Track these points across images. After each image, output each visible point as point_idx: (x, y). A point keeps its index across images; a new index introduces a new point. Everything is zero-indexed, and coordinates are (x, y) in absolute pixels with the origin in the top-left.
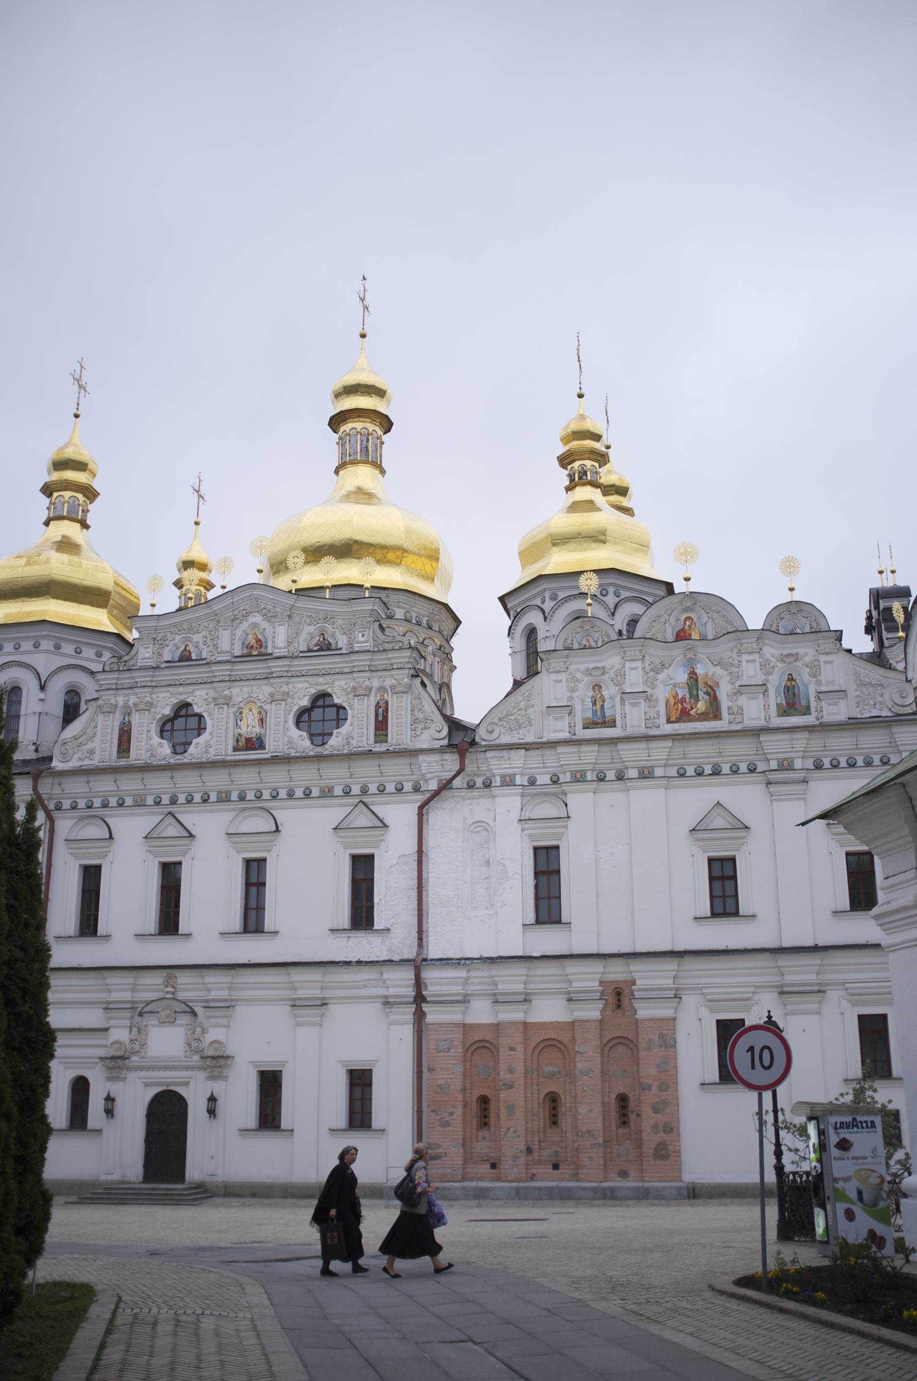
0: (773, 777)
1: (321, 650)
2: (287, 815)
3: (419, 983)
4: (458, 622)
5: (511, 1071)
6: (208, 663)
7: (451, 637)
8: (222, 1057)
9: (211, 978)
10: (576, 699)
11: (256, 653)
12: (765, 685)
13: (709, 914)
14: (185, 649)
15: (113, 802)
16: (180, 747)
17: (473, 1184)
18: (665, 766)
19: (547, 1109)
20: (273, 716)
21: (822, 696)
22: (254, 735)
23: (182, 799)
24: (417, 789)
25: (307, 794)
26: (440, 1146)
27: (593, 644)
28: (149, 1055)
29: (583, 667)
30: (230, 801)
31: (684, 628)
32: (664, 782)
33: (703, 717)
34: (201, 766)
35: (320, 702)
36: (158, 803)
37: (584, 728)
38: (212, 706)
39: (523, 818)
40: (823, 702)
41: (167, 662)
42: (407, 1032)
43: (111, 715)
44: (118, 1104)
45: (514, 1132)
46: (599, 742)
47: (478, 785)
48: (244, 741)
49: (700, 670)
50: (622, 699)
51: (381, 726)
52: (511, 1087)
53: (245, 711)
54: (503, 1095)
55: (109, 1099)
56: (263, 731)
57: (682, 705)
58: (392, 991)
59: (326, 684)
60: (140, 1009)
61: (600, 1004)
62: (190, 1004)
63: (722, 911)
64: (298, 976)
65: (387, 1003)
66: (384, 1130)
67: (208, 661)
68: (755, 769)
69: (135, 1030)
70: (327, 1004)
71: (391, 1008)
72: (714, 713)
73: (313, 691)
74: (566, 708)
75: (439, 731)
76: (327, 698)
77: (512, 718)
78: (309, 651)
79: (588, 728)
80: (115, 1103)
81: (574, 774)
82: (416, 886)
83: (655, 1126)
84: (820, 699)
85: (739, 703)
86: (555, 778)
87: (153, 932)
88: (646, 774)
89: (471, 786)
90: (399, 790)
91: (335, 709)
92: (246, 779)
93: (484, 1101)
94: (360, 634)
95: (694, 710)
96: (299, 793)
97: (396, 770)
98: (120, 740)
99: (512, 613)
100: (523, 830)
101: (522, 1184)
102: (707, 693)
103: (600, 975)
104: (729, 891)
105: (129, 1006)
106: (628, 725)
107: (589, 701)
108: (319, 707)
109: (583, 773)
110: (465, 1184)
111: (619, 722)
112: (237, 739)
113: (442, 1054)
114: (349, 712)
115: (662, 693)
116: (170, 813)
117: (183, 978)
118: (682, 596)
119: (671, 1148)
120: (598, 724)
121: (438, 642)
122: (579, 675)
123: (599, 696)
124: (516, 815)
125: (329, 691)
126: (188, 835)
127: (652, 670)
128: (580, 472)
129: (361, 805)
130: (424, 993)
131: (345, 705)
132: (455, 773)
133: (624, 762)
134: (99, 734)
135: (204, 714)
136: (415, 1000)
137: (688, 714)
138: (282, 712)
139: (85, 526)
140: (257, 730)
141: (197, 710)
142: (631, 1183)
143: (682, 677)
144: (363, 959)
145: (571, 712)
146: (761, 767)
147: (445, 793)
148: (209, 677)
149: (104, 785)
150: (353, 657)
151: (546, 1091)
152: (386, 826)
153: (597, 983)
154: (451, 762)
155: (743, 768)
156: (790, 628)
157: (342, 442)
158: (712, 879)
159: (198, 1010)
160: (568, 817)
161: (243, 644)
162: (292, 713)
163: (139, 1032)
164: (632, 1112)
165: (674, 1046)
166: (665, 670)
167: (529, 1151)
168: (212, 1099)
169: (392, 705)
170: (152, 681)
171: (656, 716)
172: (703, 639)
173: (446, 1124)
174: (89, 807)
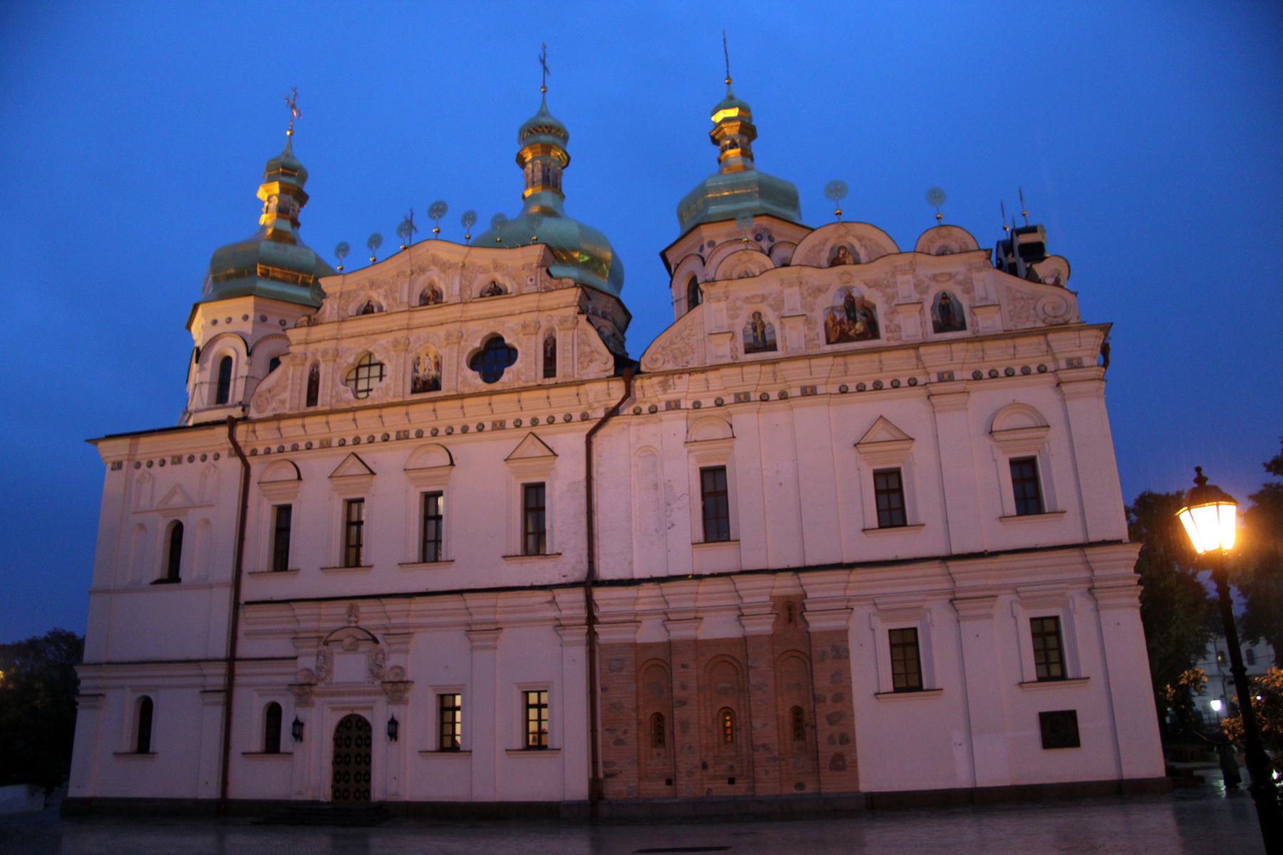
0: (934, 389)
2: (464, 448)
3: (590, 603)
5: (684, 687)
8: (402, 682)
9: (392, 606)
12: (920, 303)
13: (876, 525)
14: (368, 304)
15: (302, 445)
21: (977, 311)
23: (364, 439)
24: (585, 418)
25: (481, 428)
27: (751, 275)
28: (334, 681)
32: (826, 399)
33: (861, 337)
36: (342, 443)
38: (392, 353)
39: (688, 440)
42: (580, 653)
45: (690, 748)
47: (643, 412)
48: (421, 383)
49: (855, 294)
50: (781, 323)
53: (423, 356)
54: (676, 712)
56: (439, 374)
57: (841, 327)
58: (565, 613)
60: (324, 639)
61: (772, 619)
62: (372, 632)
64: (472, 600)
65: (559, 625)
66: (559, 749)
69: (321, 657)
70: (501, 629)
71: (564, 629)
72: (872, 330)
73: (486, 333)
74: (728, 335)
75: (606, 363)
77: (674, 346)
78: (481, 296)
81: (737, 396)
82: (585, 511)
83: (831, 740)
84: (974, 314)
85: (896, 322)
86: (719, 402)
87: (337, 565)
88: (809, 392)
89: (637, 412)
90: (568, 419)
92: (422, 415)
93: (659, 718)
94: (529, 279)
95: (853, 331)
96: (473, 428)
97: (563, 401)
100: (689, 452)
102: (864, 315)
104: (895, 504)
105: (314, 635)
106: (789, 348)
107: (750, 327)
109: (747, 395)
111: (779, 346)
113: (615, 673)
115: (820, 317)
116: (353, 453)
117: (365, 607)
123: (759, 322)
124: (682, 437)
126: (367, 472)
127: (810, 295)
129: (531, 436)
130: (596, 614)
132: (619, 401)
133: (786, 382)
134: (290, 386)
135: (385, 361)
138: (455, 354)
139: (295, 223)
140: (433, 372)
144: (535, 584)
145: (732, 339)
147: (614, 420)
152: (556, 455)
153: (767, 598)
154: (618, 389)
158: (878, 492)
159: (379, 637)
160: (734, 437)
162: (466, 354)
164: (806, 725)
165: (847, 657)
166: (822, 295)
167: (705, 766)
168: (393, 723)
171: (816, 337)
172: (857, 262)
173: (619, 742)
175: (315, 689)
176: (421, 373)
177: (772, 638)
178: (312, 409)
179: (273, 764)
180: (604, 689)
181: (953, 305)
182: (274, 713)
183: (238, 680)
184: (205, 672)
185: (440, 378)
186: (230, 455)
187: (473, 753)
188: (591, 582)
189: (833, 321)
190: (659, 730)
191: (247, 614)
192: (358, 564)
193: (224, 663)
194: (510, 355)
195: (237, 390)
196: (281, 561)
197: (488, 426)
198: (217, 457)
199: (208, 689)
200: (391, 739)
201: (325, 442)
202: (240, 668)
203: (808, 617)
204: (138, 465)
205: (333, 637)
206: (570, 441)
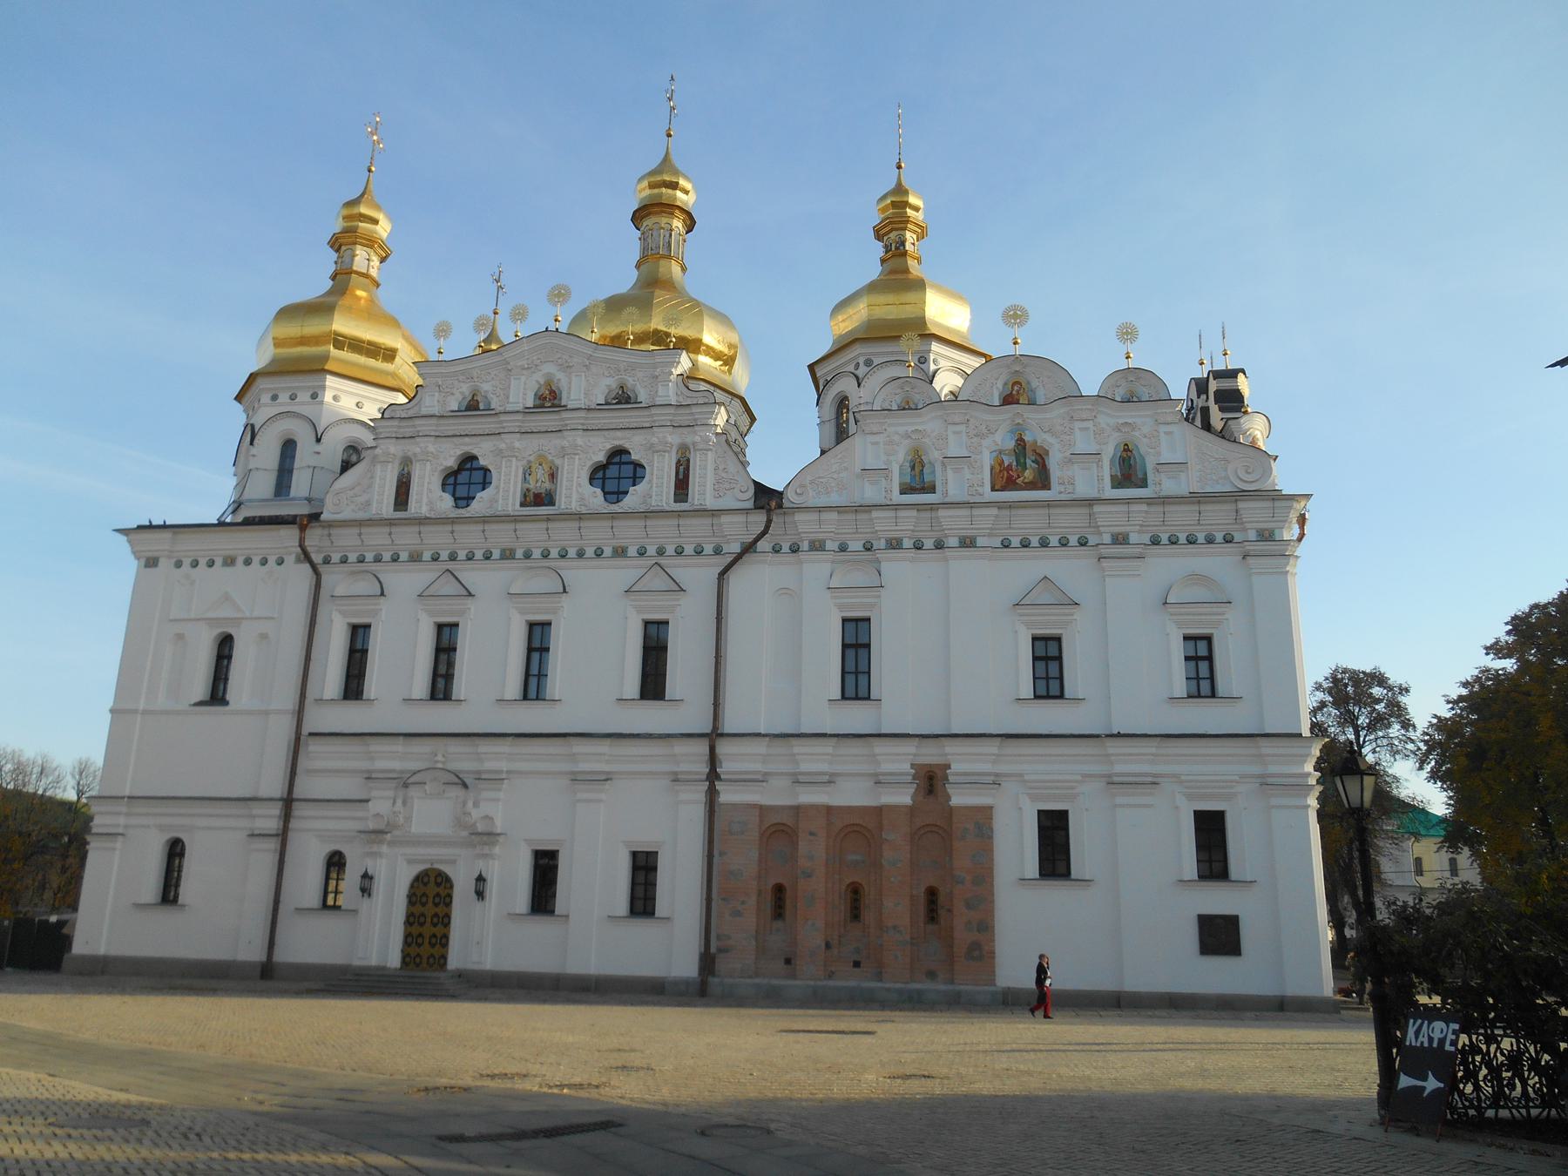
0: (1104, 551)
1: (616, 404)
2: (579, 575)
3: (713, 759)
4: (753, 419)
7: (746, 435)
8: (490, 834)
9: (485, 747)
10: (894, 463)
11: (549, 405)
15: (387, 556)
16: (463, 500)
17: (765, 981)
18: (990, 535)
20: (565, 472)
22: (543, 491)
23: (462, 555)
24: (718, 551)
25: (599, 553)
27: (913, 406)
29: (901, 429)
30: (514, 559)
31: (1011, 393)
33: (1031, 486)
34: (484, 520)
35: (617, 459)
36: (435, 558)
41: (453, 411)
44: (376, 880)
46: (918, 507)
48: (532, 498)
49: (1028, 438)
50: (943, 464)
51: (682, 486)
52: (809, 876)
53: (534, 466)
55: (366, 877)
56: (553, 487)
57: (1008, 473)
58: (684, 767)
59: (622, 439)
62: (461, 776)
63: (1045, 694)
64: (580, 747)
65: (676, 779)
66: (668, 918)
67: (498, 412)
68: (1087, 542)
69: (399, 802)
70: (611, 779)
72: (1042, 480)
73: (609, 446)
76: (623, 456)
78: (607, 404)
79: (905, 494)
80: (373, 881)
88: (968, 543)
89: (776, 550)
90: (699, 552)
91: (632, 466)
92: (533, 535)
96: (590, 552)
97: (696, 530)
101: (819, 983)
103: (912, 757)
104: (1054, 672)
107: (908, 465)
110: (757, 981)
112: (525, 494)
115: (987, 461)
116: (448, 570)
118: (1013, 358)
122: (896, 438)
123: (918, 460)
126: (465, 593)
128: (897, 243)
131: (644, 462)
136: (707, 777)
137: (1014, 483)
140: (547, 485)
141: (482, 462)
143: (1011, 444)
146: (1092, 540)
148: (497, 428)
149: (377, 539)
150: (654, 411)
151: (848, 881)
153: (906, 767)
155: (1073, 540)
157: (643, 239)
158: (1035, 659)
161: (535, 395)
162: (586, 468)
163: (404, 803)
167: (828, 946)
168: (480, 879)
169: (695, 463)
170: (435, 431)
172: (1032, 403)
173: (737, 913)
174: (362, 562)
175: (388, 837)
176: (532, 486)
177: (912, 811)
179: (329, 924)
180: (721, 854)
181: (1135, 458)
182: (336, 862)
183: (293, 824)
184: (255, 812)
185: (556, 491)
186: (298, 561)
188: (714, 736)
189: (1000, 465)
190: (779, 901)
191: (313, 748)
192: (447, 697)
193: (281, 803)
194: (637, 472)
195: (300, 484)
196: (353, 686)
197: (608, 551)
198: (280, 562)
199: (256, 832)
200: (478, 899)
202: (299, 810)
203: (950, 790)
204: (179, 564)
206: (699, 577)
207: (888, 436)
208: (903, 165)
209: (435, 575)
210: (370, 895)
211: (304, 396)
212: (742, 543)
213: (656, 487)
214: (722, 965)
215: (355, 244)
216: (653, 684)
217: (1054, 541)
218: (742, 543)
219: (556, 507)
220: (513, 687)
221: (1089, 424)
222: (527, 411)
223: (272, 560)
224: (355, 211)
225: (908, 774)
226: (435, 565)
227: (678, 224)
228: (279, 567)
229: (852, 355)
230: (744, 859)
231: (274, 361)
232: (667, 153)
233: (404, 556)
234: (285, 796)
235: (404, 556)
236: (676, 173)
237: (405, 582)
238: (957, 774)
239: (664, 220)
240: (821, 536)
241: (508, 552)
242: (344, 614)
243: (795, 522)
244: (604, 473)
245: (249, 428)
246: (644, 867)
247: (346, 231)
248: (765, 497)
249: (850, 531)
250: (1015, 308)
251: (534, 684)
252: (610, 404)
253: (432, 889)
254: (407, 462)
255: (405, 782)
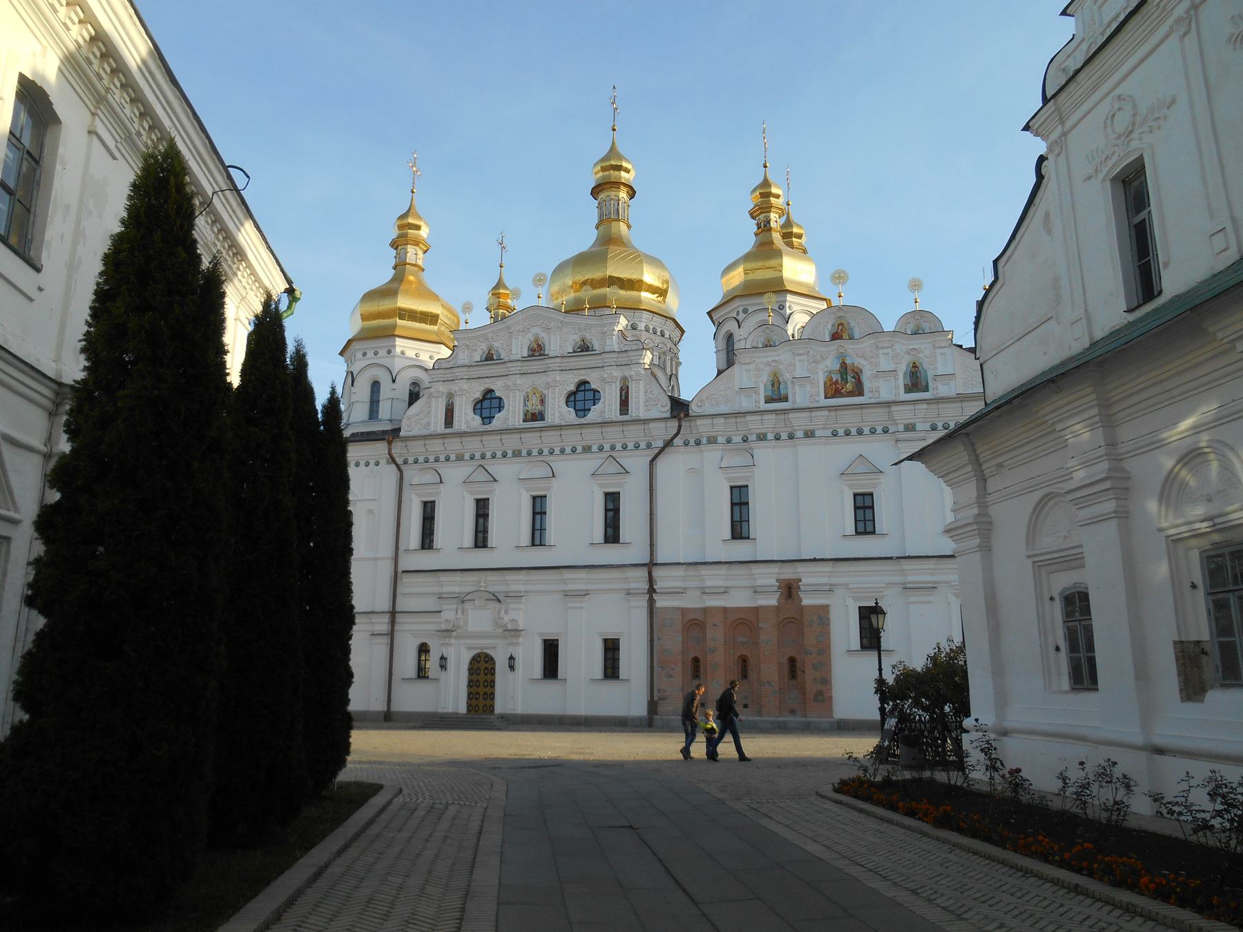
0: (899, 436)
1: (582, 351)
2: (559, 464)
3: (651, 580)
4: (683, 332)
6: (504, 362)
8: (516, 630)
9: (510, 576)
10: (760, 383)
11: (538, 354)
15: (442, 458)
16: (487, 419)
18: (824, 428)
19: (740, 666)
23: (488, 455)
24: (649, 446)
26: (665, 691)
27: (772, 344)
29: (764, 360)
32: (823, 440)
33: (851, 394)
35: (582, 388)
36: (472, 458)
37: (766, 403)
40: (938, 383)
43: (440, 398)
44: (449, 660)
48: (530, 415)
50: (792, 382)
51: (624, 404)
52: (714, 652)
55: (443, 658)
57: (835, 385)
58: (633, 585)
61: (777, 595)
62: (496, 595)
63: (863, 531)
64: (568, 575)
65: (628, 593)
66: (627, 680)
68: (888, 431)
69: (460, 612)
72: (859, 390)
73: (576, 380)
78: (574, 352)
86: (745, 439)
88: (809, 434)
89: (686, 444)
95: (844, 389)
96: (568, 450)
97: (634, 434)
98: (446, 415)
99: (716, 323)
104: (869, 516)
108: (582, 391)
114: (602, 394)
115: (821, 379)
119: (826, 694)
120: (776, 400)
121: (669, 346)
125: (588, 379)
127: (814, 362)
131: (598, 389)
140: (539, 407)
141: (498, 394)
142: (798, 719)
143: (837, 367)
149: (436, 446)
150: (604, 356)
153: (774, 582)
156: (915, 329)
157: (600, 207)
158: (856, 508)
163: (463, 613)
168: (511, 658)
169: (632, 389)
172: (851, 338)
173: (670, 676)
174: (427, 462)
175: (454, 633)
176: (530, 408)
178: (449, 431)
179: (423, 687)
181: (920, 372)
182: (423, 649)
183: (397, 627)
184: (373, 621)
186: (388, 463)
187: (568, 681)
188: (651, 565)
190: (696, 668)
191: (406, 580)
192: (485, 546)
193: (389, 615)
194: (595, 396)
195: (384, 411)
196: (427, 540)
197: (579, 449)
198: (377, 464)
199: (375, 633)
201: (460, 456)
202: (399, 618)
205: (466, 598)
206: (637, 463)
207: (756, 365)
208: (768, 165)
209: (472, 469)
210: (445, 669)
211: (383, 353)
212: (664, 440)
213: (608, 406)
214: (660, 709)
215: (407, 244)
216: (612, 534)
217: (866, 430)
218: (664, 440)
219: (545, 422)
220: (525, 539)
221: (889, 350)
222: (524, 360)
223: (372, 463)
224: (405, 221)
225: (773, 586)
226: (473, 462)
227: (623, 194)
228: (377, 467)
229: (734, 306)
230: (673, 642)
231: (362, 330)
232: (613, 143)
233: (453, 457)
234: (391, 610)
235: (453, 457)
236: (620, 158)
237: (455, 474)
238: (805, 585)
239: (613, 194)
240: (714, 434)
241: (517, 452)
242: (419, 495)
243: (697, 426)
244: (575, 398)
245: (349, 373)
246: (611, 648)
247: (400, 236)
248: (679, 408)
249: (734, 429)
250: (839, 272)
251: (538, 537)
252: (576, 352)
253: (482, 665)
254: (450, 396)
255: (462, 599)
